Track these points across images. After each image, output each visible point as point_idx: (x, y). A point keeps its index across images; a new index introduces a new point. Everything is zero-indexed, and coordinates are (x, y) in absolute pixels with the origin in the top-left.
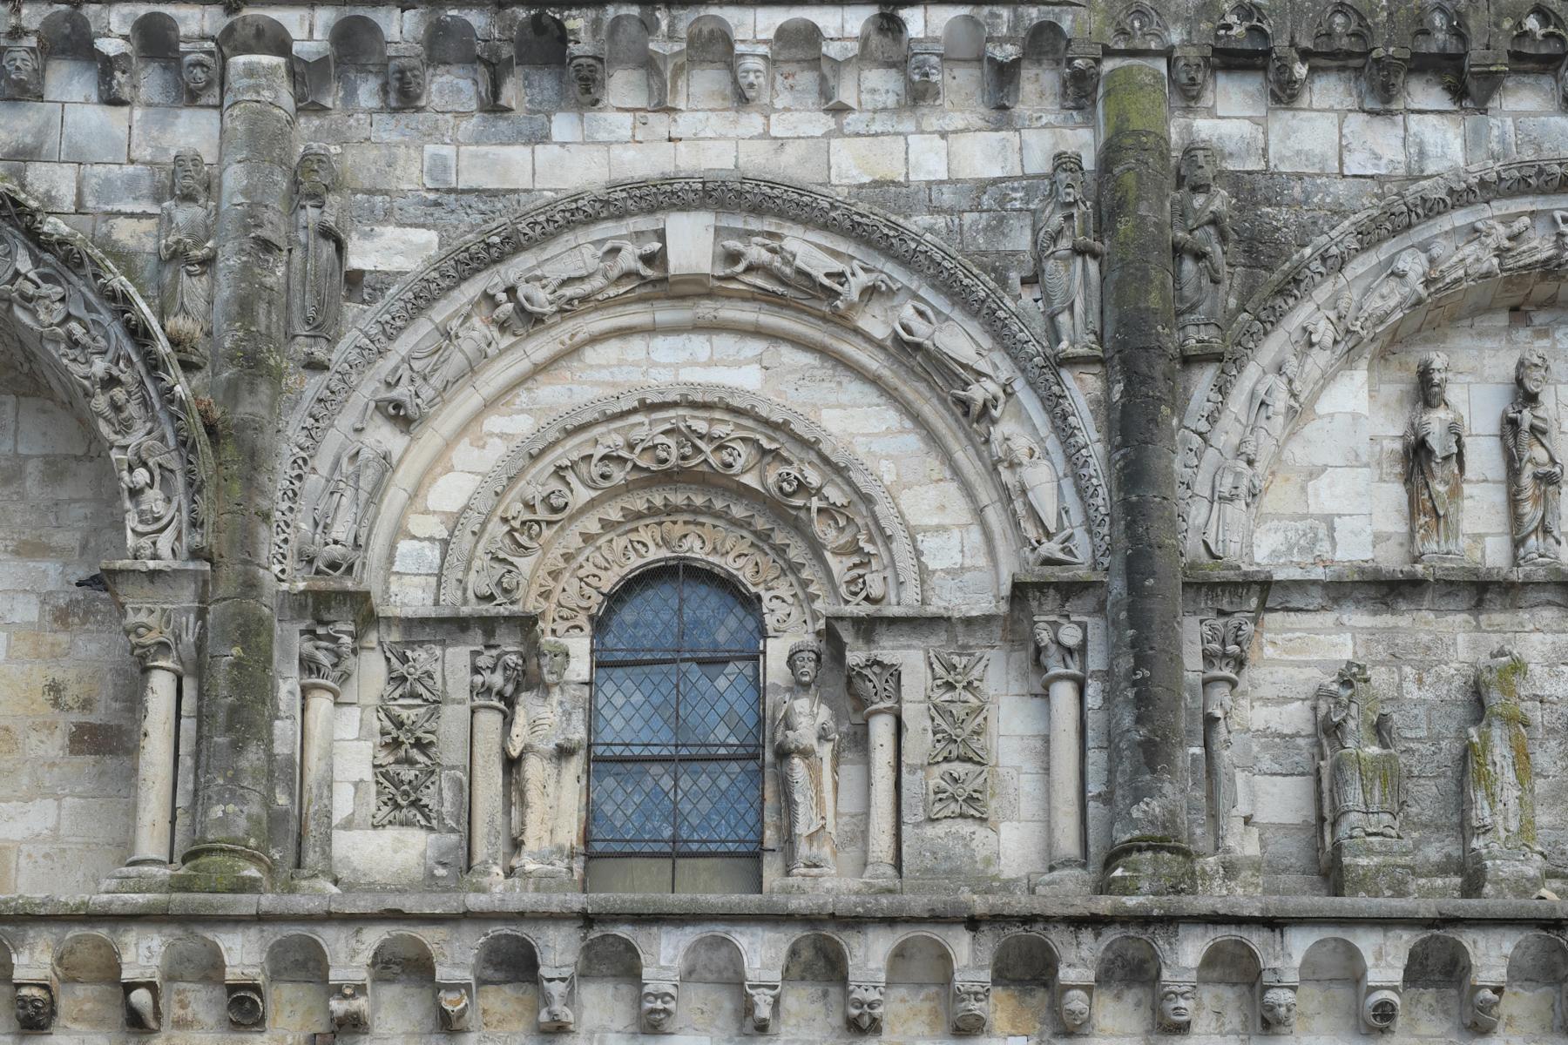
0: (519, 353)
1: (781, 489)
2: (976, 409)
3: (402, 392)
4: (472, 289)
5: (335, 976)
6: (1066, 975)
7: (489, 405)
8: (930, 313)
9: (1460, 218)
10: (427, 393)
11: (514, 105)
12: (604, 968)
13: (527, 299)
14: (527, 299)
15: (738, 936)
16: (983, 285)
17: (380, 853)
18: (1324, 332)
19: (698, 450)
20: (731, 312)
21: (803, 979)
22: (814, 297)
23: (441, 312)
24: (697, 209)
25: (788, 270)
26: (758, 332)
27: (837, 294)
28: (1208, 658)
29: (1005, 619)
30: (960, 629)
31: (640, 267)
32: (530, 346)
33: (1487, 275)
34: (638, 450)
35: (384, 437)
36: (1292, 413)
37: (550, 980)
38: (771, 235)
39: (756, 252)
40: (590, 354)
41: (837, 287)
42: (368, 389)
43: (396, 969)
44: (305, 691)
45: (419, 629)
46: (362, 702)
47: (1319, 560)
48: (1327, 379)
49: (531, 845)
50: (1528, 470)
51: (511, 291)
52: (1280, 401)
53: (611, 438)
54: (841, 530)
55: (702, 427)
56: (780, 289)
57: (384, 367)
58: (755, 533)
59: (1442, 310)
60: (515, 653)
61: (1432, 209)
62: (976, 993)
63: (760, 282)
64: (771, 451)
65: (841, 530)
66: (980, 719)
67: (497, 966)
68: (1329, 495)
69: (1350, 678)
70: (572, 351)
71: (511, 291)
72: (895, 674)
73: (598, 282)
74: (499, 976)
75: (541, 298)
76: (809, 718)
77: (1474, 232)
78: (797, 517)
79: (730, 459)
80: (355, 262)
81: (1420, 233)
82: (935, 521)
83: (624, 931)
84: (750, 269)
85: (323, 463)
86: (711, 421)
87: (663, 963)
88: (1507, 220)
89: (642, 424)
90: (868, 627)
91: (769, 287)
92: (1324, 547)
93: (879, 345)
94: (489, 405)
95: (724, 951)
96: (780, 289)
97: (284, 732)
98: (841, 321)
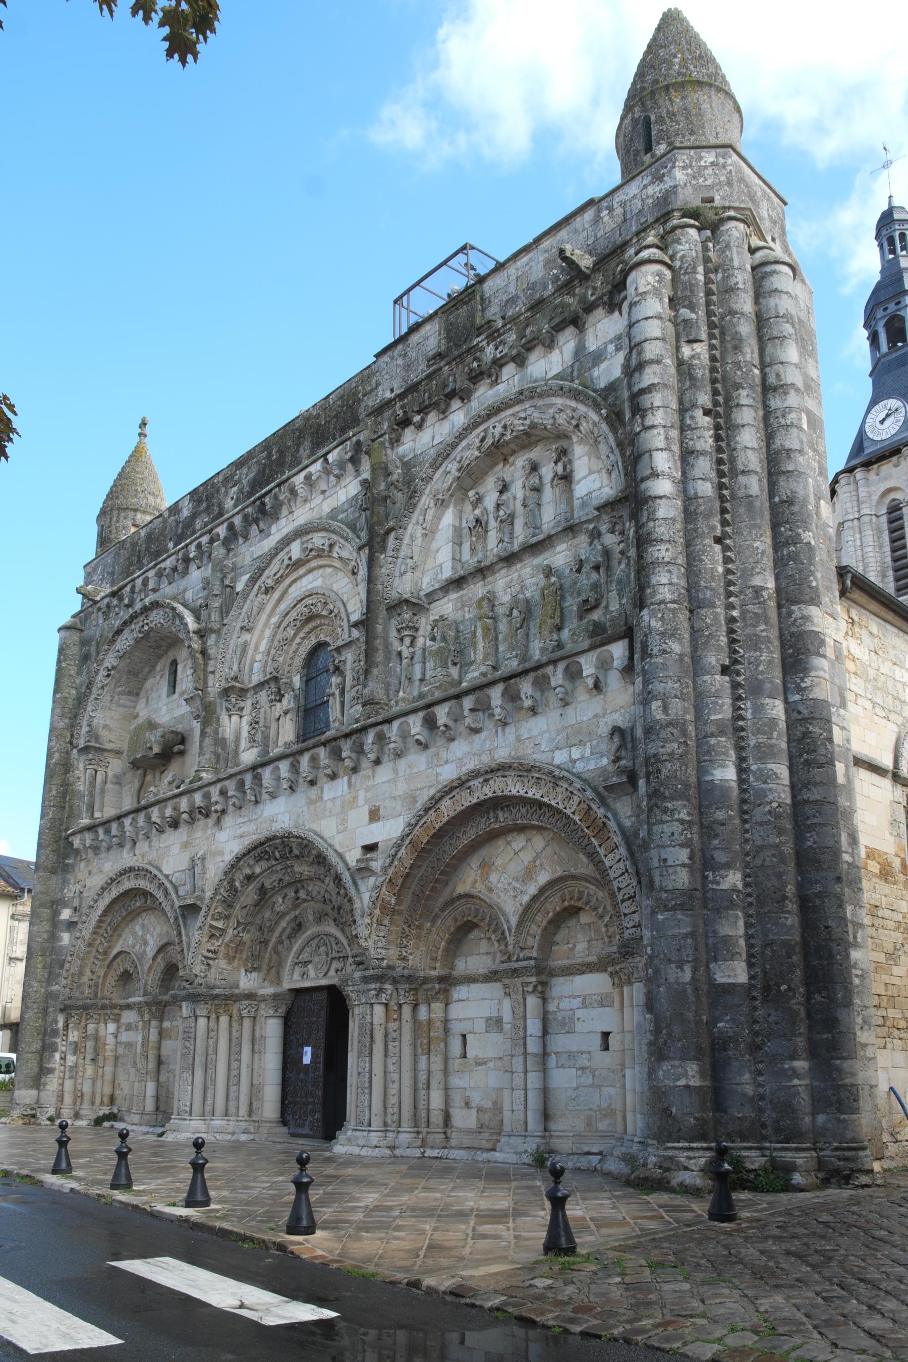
9: (464, 443)
20: (314, 564)
28: (399, 631)
33: (477, 458)
35: (246, 636)
40: (291, 590)
47: (439, 581)
48: (438, 518)
53: (293, 614)
59: (470, 477)
61: (453, 446)
70: (285, 591)
75: (270, 582)
77: (468, 447)
81: (452, 457)
88: (477, 436)
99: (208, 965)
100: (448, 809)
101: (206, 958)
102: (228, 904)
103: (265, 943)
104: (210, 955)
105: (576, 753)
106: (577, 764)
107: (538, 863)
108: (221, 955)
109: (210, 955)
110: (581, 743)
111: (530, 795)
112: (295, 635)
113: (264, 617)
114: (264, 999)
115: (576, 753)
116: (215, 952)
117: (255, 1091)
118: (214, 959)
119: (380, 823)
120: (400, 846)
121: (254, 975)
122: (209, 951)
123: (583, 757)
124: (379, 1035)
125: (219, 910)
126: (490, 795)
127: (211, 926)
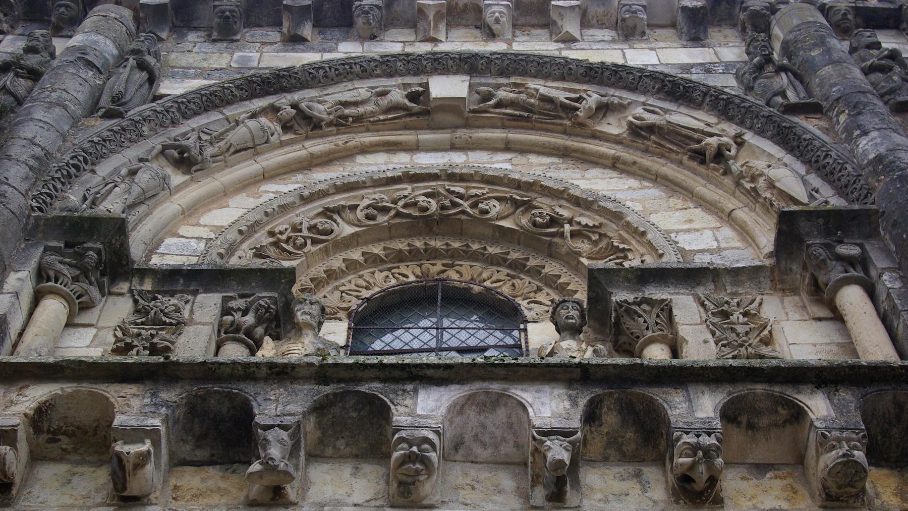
0: (298, 146)
1: (535, 224)
2: (710, 153)
8: (657, 110)
10: (209, 151)
11: (309, 39)
12: (341, 444)
13: (309, 108)
14: (309, 108)
15: (519, 393)
19: (459, 205)
21: (605, 459)
22: (555, 117)
24: (456, 73)
25: (532, 101)
27: (577, 109)
29: (772, 269)
30: (727, 279)
31: (406, 101)
32: (307, 144)
34: (401, 203)
37: (267, 428)
38: (516, 85)
39: (502, 94)
41: (577, 105)
43: (65, 442)
46: (101, 324)
54: (595, 243)
56: (526, 114)
58: (510, 266)
60: (270, 298)
62: (848, 440)
63: (508, 111)
64: (523, 203)
65: (595, 243)
66: (766, 332)
67: (200, 440)
73: (369, 108)
74: (200, 454)
75: (320, 110)
78: (550, 244)
79: (487, 207)
82: (686, 227)
83: (374, 387)
84: (500, 105)
86: (467, 188)
87: (419, 412)
89: (406, 189)
91: (517, 113)
93: (616, 140)
95: (501, 414)
96: (526, 114)
98: (580, 129)
112: (352, 241)
113: (247, 168)
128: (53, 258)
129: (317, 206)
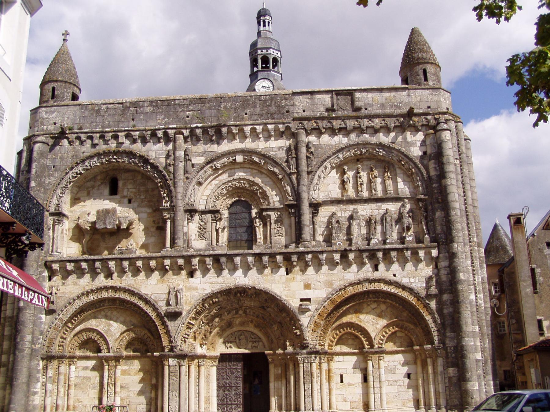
3: (200, 180)
4: (209, 165)
5: (193, 264)
6: (293, 259)
7: (213, 180)
16: (280, 162)
17: (198, 244)
18: (329, 166)
23: (205, 169)
26: (249, 168)
36: (324, 177)
42: (195, 181)
44: (188, 223)
45: (203, 212)
49: (220, 242)
50: (359, 183)
51: (215, 165)
52: (322, 176)
55: (242, 182)
57: (198, 177)
68: (330, 188)
69: (333, 214)
71: (215, 165)
72: (270, 216)
75: (219, 166)
76: (258, 223)
80: (193, 162)
85: (190, 191)
90: (267, 210)
92: (330, 196)
94: (213, 180)
97: (185, 230)
99: (185, 342)
100: (351, 291)
101: (184, 338)
102: (198, 313)
103: (211, 332)
104: (187, 336)
105: (412, 280)
106: (413, 284)
107: (383, 314)
108: (190, 336)
109: (187, 336)
110: (414, 277)
111: (392, 291)
113: (210, 179)
114: (211, 358)
115: (412, 280)
116: (188, 335)
117: (208, 400)
118: (187, 338)
119: (312, 291)
120: (326, 301)
121: (204, 347)
122: (186, 334)
123: (415, 282)
124: (315, 375)
125: (193, 316)
126: (373, 288)
127: (189, 323)
128: (189, 217)
129: (221, 188)
